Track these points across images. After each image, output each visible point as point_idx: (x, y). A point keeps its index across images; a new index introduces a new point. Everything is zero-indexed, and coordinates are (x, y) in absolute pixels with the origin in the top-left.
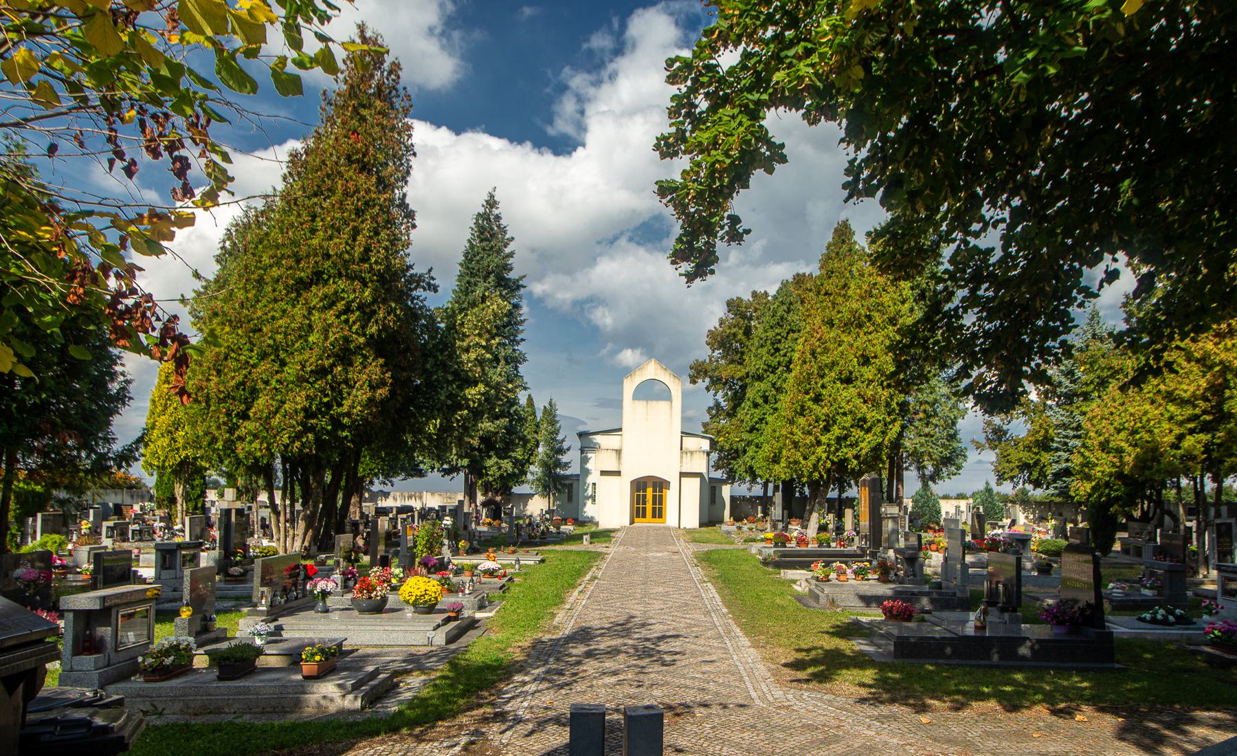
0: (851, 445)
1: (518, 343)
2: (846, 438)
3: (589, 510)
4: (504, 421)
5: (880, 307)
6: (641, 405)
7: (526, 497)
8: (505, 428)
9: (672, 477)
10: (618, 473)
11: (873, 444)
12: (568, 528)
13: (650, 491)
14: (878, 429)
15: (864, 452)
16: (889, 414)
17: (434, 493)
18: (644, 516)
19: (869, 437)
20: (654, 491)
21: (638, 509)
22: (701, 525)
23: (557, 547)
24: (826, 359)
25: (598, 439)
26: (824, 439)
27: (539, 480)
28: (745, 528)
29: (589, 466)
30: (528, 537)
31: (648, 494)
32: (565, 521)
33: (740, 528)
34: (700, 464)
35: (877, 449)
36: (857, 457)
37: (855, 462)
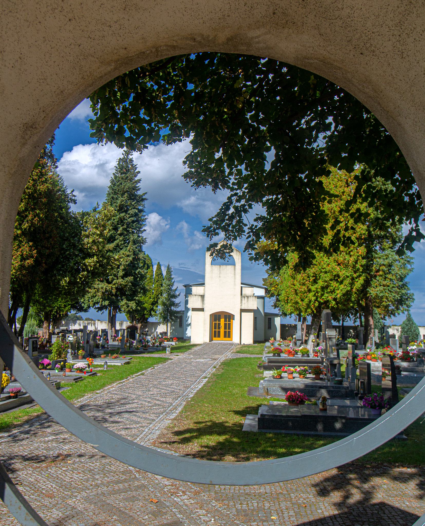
2: (327, 287)
7: (156, 325)
13: (222, 320)
15: (338, 296)
18: (219, 336)
20: (225, 321)
21: (215, 332)
31: (221, 323)
37: (334, 303)
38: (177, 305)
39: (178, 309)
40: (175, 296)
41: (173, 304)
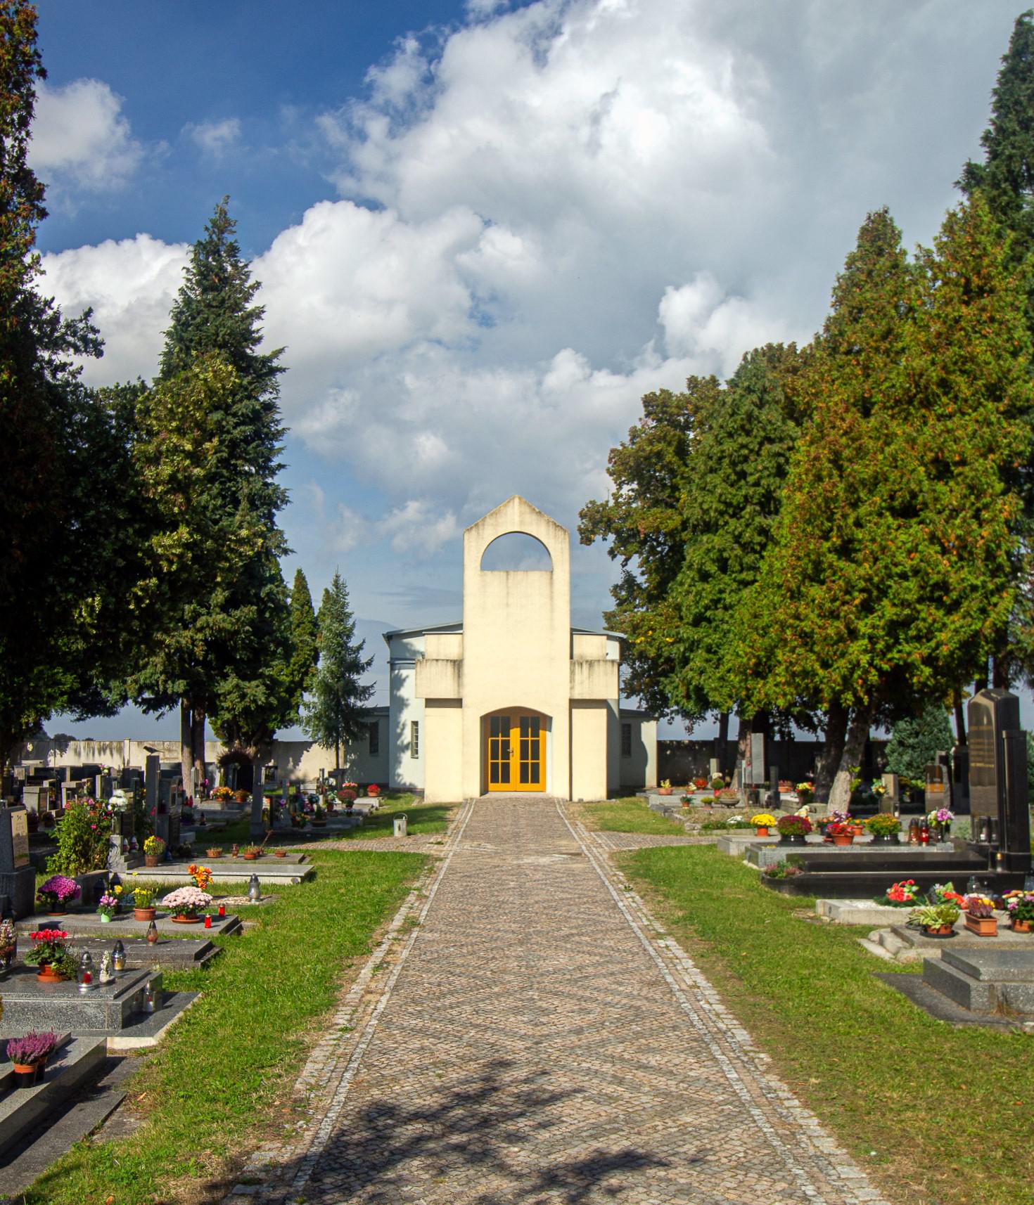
0: (918, 638)
1: (273, 473)
2: (906, 623)
3: (408, 771)
4: (249, 611)
5: (966, 365)
6: (495, 579)
7: (298, 749)
8: (251, 622)
9: (552, 703)
10: (457, 703)
11: (962, 636)
12: (368, 803)
13: (515, 734)
14: (971, 604)
15: (944, 650)
16: (994, 574)
17: (124, 741)
18: (506, 779)
19: (956, 620)
21: (495, 766)
22: (611, 794)
23: (344, 845)
24: (863, 470)
25: (418, 644)
26: (863, 626)
27: (318, 717)
28: (698, 798)
29: (404, 692)
30: (298, 823)
31: (512, 738)
32: (362, 790)
33: (687, 801)
34: (607, 684)
35: (970, 644)
36: (929, 660)
37: (927, 671)
38: (365, 692)
39: (369, 703)
40: (357, 667)
41: (352, 689)
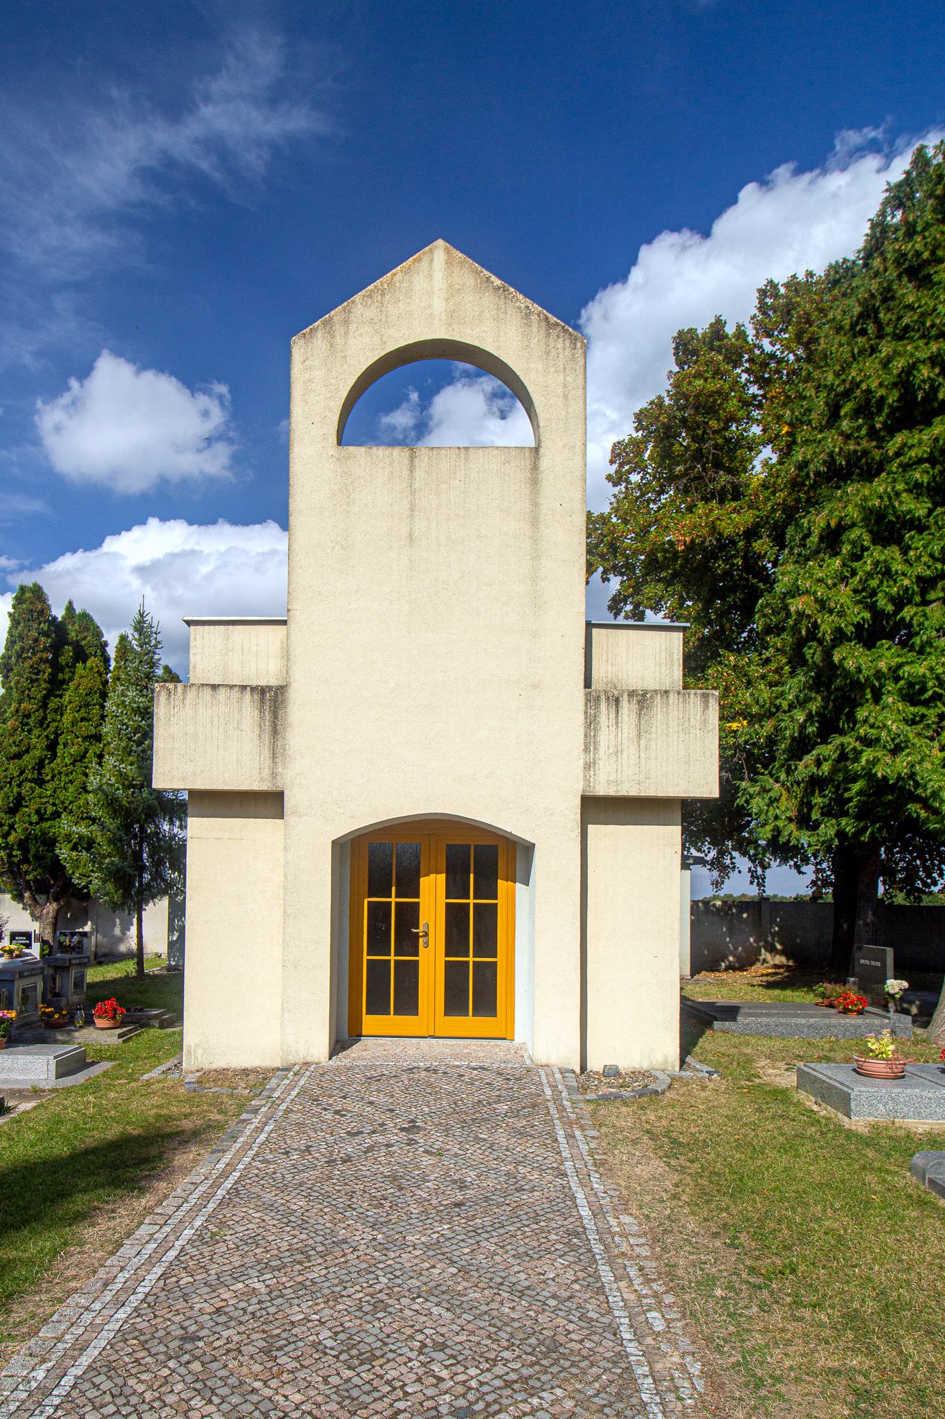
6: (377, 466)
10: (269, 803)
13: (433, 894)
18: (408, 1003)
20: (455, 887)
31: (422, 901)
